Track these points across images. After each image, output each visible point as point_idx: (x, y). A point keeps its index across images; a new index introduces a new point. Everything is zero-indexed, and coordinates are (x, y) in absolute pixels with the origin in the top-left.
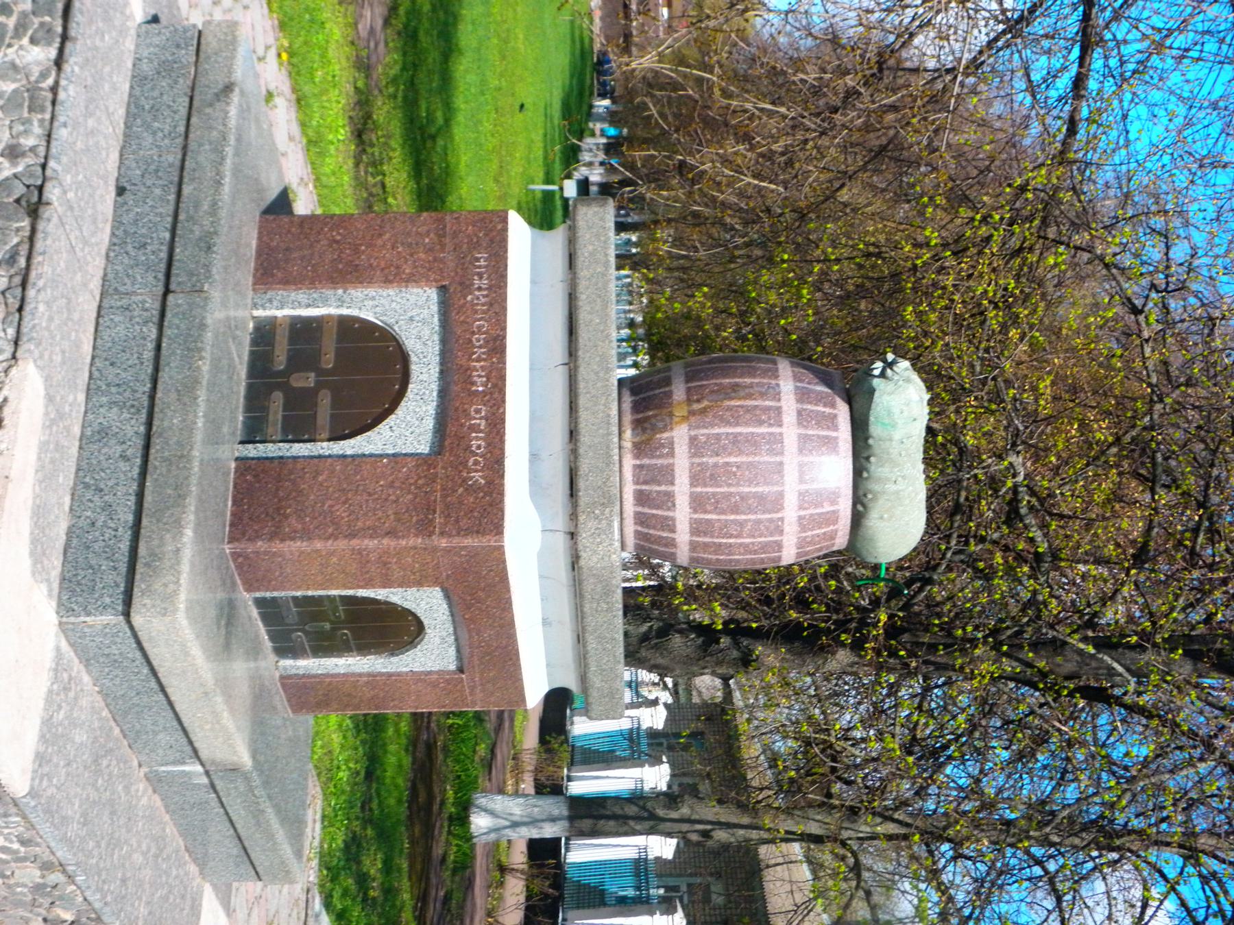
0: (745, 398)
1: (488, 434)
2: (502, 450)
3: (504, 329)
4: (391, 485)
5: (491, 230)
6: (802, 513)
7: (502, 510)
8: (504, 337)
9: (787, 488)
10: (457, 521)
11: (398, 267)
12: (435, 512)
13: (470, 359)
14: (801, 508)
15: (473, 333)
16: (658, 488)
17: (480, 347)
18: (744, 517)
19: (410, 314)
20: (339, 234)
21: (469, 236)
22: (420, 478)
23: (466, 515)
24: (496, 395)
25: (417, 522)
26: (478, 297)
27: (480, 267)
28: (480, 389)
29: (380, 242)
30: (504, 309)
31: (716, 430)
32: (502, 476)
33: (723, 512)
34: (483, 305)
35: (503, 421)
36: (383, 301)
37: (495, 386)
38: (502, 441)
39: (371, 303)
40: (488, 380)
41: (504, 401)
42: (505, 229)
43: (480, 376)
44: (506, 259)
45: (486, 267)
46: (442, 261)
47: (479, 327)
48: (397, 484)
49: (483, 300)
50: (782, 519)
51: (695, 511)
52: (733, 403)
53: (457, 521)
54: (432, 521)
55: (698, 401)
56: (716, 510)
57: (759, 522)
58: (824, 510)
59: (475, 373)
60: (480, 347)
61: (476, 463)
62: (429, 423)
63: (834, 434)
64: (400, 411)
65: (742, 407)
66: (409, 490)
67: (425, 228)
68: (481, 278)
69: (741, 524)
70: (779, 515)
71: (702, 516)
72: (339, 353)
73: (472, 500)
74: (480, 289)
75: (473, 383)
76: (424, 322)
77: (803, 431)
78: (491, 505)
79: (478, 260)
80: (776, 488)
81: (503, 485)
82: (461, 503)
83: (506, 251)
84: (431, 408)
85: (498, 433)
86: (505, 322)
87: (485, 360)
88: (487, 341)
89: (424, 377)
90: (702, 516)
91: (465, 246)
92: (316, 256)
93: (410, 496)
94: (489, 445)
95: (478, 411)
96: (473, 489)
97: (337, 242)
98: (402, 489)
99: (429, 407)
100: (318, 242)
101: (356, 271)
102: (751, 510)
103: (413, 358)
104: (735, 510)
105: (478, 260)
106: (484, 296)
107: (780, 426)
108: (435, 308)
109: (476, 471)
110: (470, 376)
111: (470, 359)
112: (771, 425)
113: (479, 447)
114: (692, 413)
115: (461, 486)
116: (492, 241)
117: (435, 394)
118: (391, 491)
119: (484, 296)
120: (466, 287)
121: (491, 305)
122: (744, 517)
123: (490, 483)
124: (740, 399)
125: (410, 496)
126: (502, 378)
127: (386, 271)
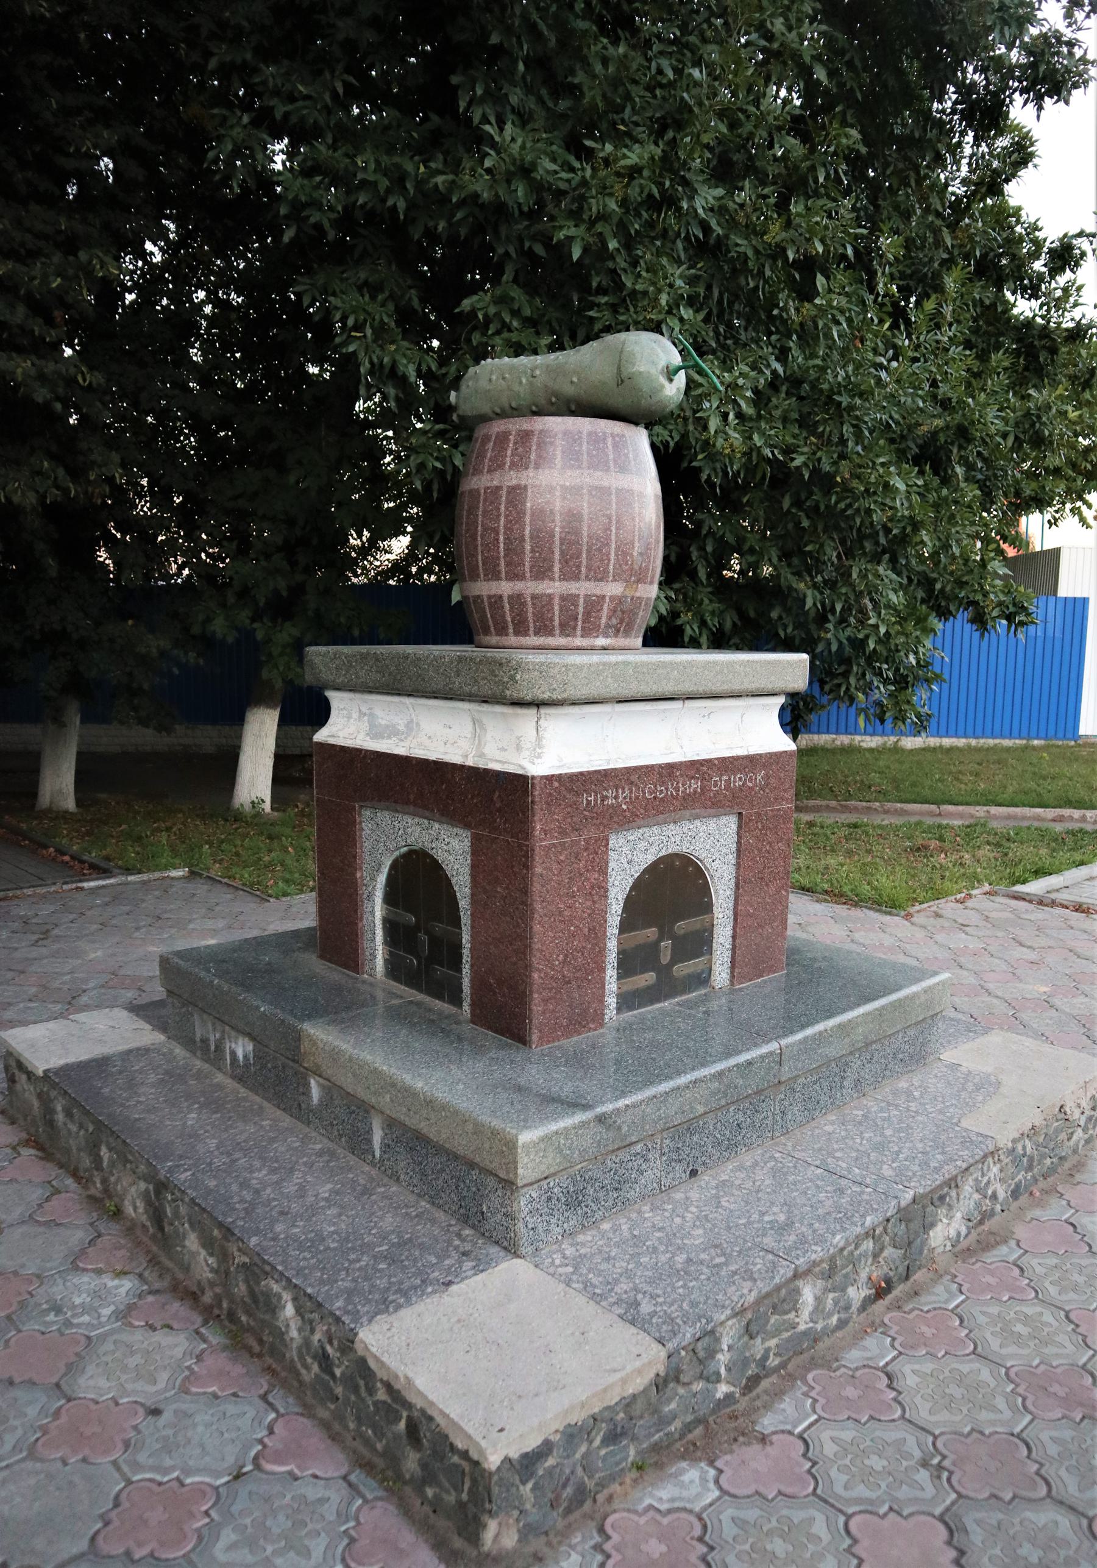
8: (660, 766)
32: (760, 755)
37: (698, 770)
46: (587, 841)
61: (751, 780)
67: (555, 866)
74: (616, 798)
75: (695, 791)
79: (589, 802)
86: (647, 767)
88: (663, 784)
89: (678, 838)
92: (578, 975)
97: (566, 956)
103: (663, 853)
105: (589, 802)
111: (675, 798)
116: (570, 790)
123: (764, 766)
126: (693, 764)
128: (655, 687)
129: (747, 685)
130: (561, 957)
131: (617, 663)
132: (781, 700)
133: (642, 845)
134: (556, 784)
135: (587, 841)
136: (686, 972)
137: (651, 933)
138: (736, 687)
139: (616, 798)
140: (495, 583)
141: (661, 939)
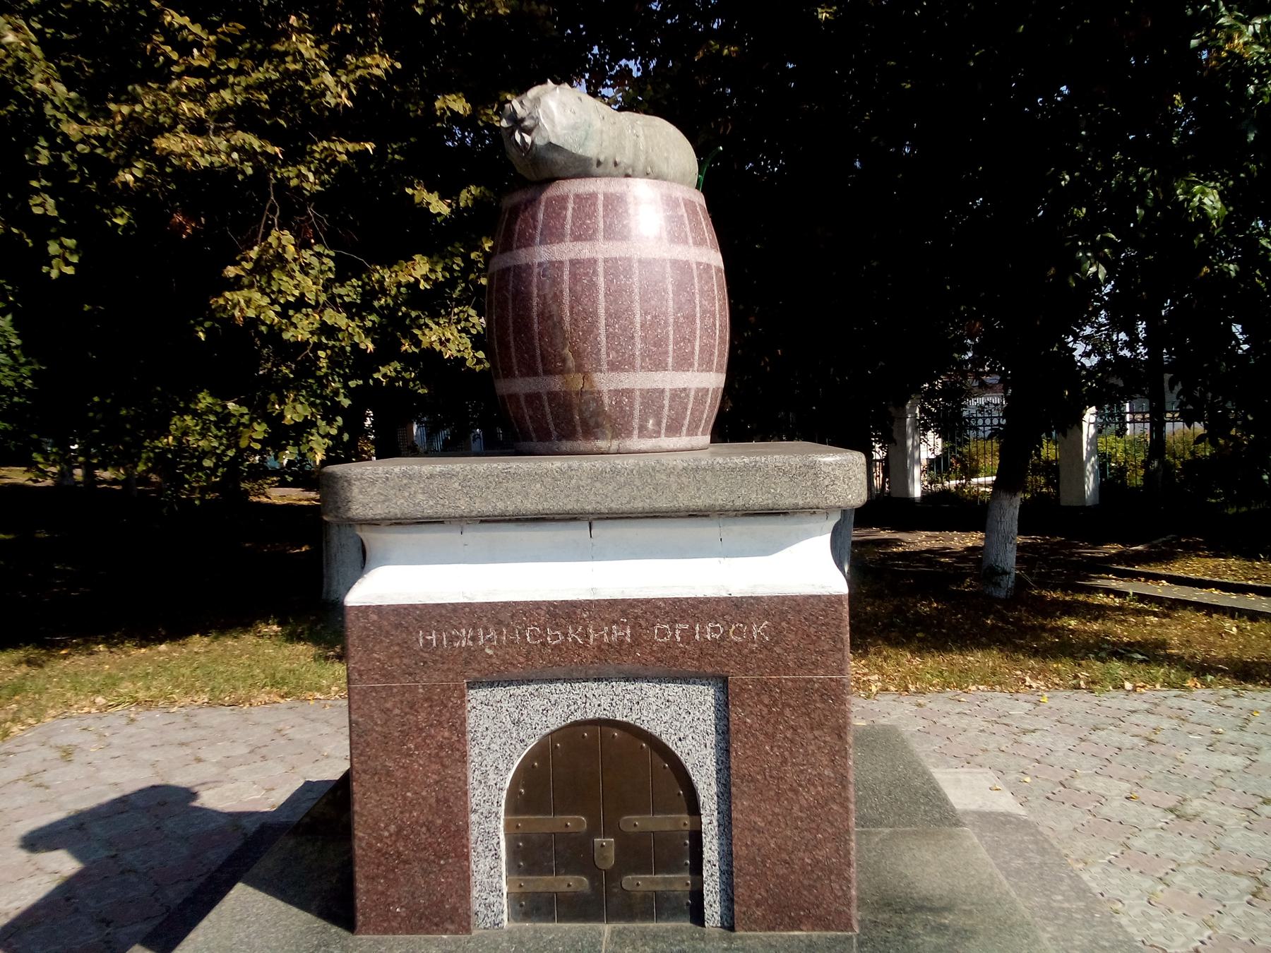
0: (561, 303)
1: (698, 620)
2: (718, 601)
3: (537, 605)
4: (771, 737)
5: (380, 628)
6: (691, 241)
7: (807, 598)
8: (550, 603)
9: (667, 256)
10: (822, 653)
11: (441, 747)
12: (811, 680)
13: (584, 647)
14: (686, 242)
15: (544, 644)
16: (666, 408)
17: (566, 635)
18: (698, 309)
19: (510, 726)
20: (387, 826)
21: (390, 658)
22: (762, 702)
23: (814, 643)
24: (638, 611)
25: (824, 701)
26: (488, 641)
27: (440, 641)
28: (628, 632)
29: (400, 774)
30: (506, 605)
31: (603, 338)
32: (758, 599)
33: (693, 332)
34: (501, 633)
35: (676, 602)
36: (489, 761)
37: (624, 613)
38: (706, 601)
39: (491, 776)
40: (614, 622)
41: (648, 601)
42: (379, 609)
43: (610, 633)
44: (425, 605)
45: (439, 632)
46: (429, 689)
47: (534, 637)
48: (770, 729)
49: (492, 633)
50: (699, 264)
51: (691, 365)
52: (567, 318)
53: (822, 653)
54: (822, 683)
55: (564, 361)
56: (691, 342)
57: (702, 292)
58: (685, 215)
59: (606, 639)
60: (566, 635)
61: (738, 632)
62: (673, 690)
63: (601, 197)
64: (656, 729)
65: (572, 308)
66: (778, 713)
68: (457, 637)
69: (704, 312)
70: (694, 266)
71: (697, 357)
72: (563, 808)
73: (792, 636)
75: (621, 641)
76: (521, 707)
77: (601, 235)
78: (799, 611)
80: (668, 269)
81: (771, 598)
82: (796, 649)
83: (414, 607)
84: (651, 690)
85: (694, 606)
86: (526, 603)
87: (585, 627)
89: (605, 702)
90: (697, 357)
91: (406, 661)
93: (787, 712)
94: (712, 618)
95: (663, 633)
96: (777, 634)
97: (400, 830)
98: (777, 722)
99: (651, 693)
100: (399, 854)
101: (447, 800)
102: (691, 301)
103: (578, 716)
104: (691, 319)
106: (486, 632)
107: (595, 261)
108: (499, 692)
109: (751, 632)
110: (609, 645)
111: (584, 647)
112: (595, 273)
113: (715, 630)
114: (579, 368)
115: (771, 650)
116: (398, 626)
117: (630, 687)
118: (781, 736)
119: (486, 632)
120: (471, 655)
121: (500, 622)
122: (698, 309)
123: (767, 615)
124: (562, 310)
125: (787, 712)
126: (612, 603)
127: (447, 762)
128: (500, 505)
129: (684, 501)
130: (393, 828)
131: (431, 476)
132: (835, 518)
133: (537, 703)
134: (374, 617)
135: (429, 689)
136: (643, 887)
137: (576, 822)
138: (663, 503)
139: (474, 639)
140: (531, 380)
141: (593, 831)
